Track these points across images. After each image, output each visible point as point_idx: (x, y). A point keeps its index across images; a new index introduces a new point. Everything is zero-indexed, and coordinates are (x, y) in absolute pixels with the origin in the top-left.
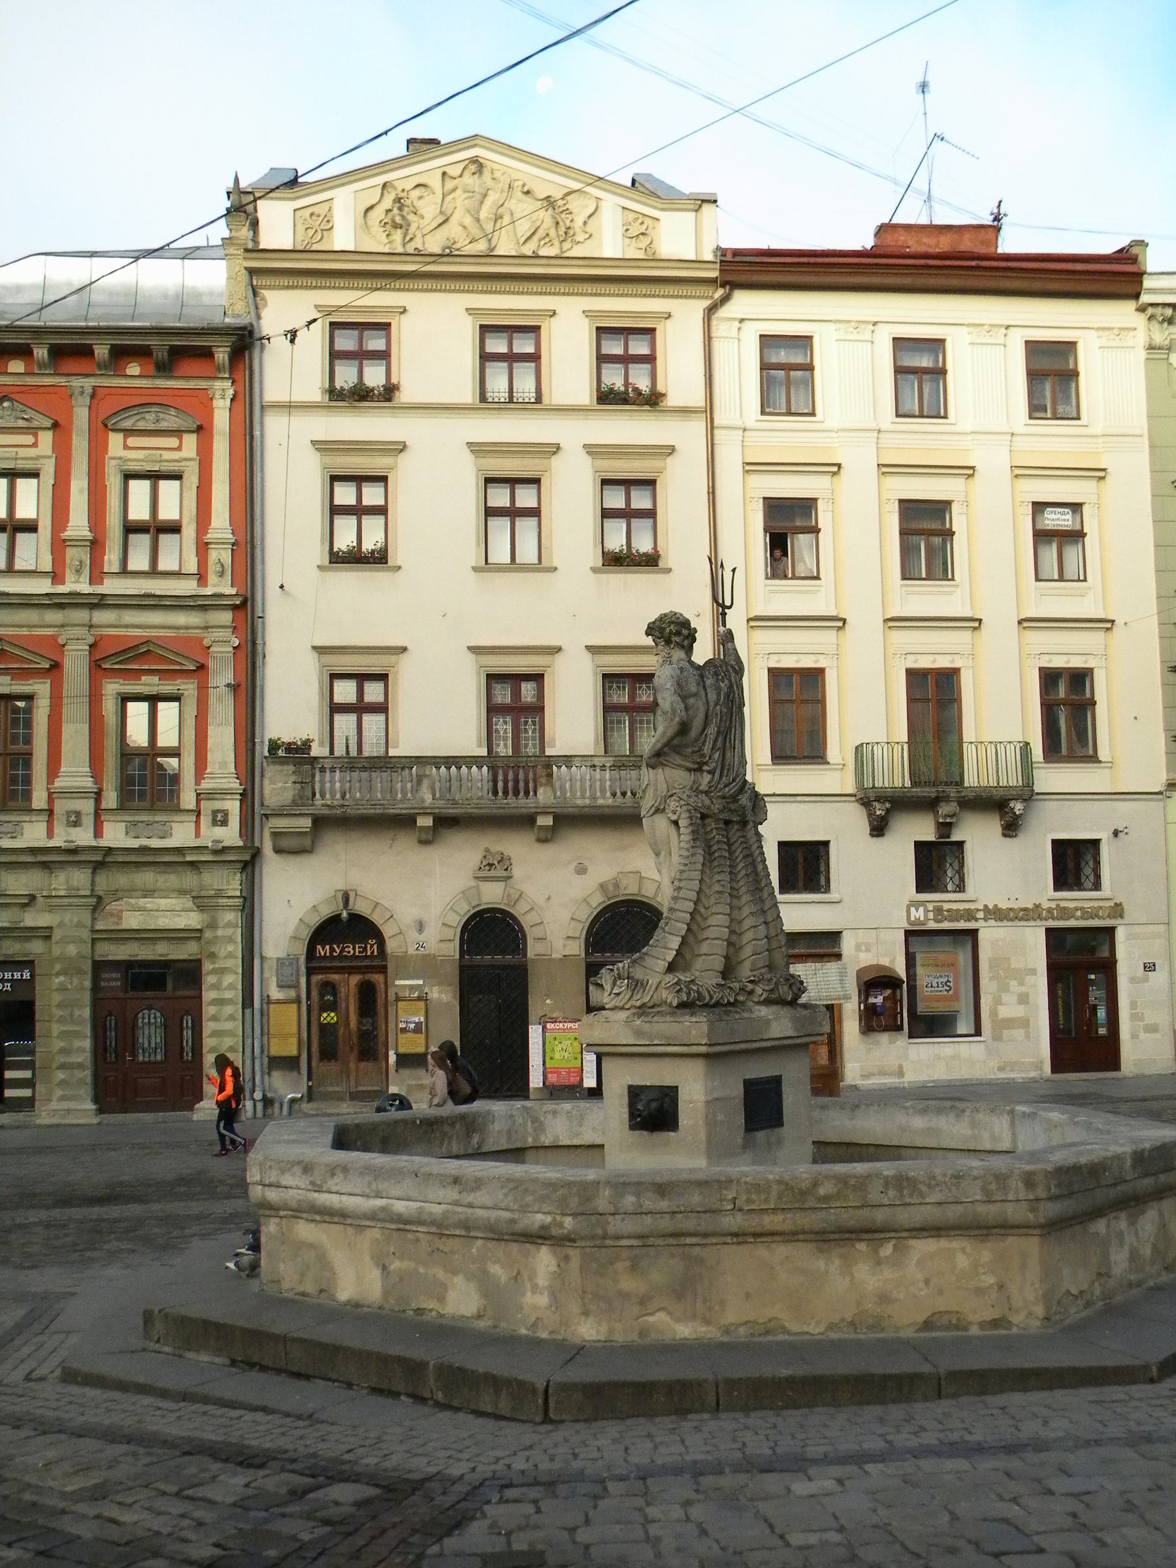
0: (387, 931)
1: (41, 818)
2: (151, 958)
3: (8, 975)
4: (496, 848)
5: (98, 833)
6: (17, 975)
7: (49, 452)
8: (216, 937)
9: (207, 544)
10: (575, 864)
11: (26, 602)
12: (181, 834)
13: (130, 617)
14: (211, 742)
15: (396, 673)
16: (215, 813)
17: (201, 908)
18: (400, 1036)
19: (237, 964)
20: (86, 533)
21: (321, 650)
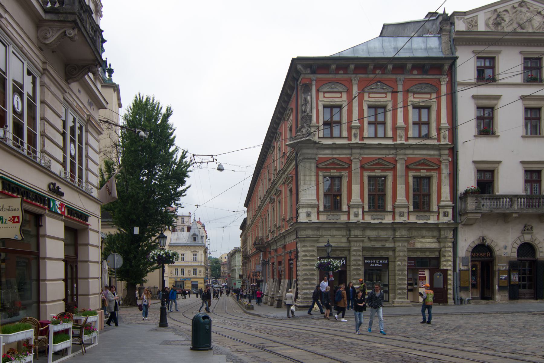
0: (496, 249)
1: (391, 214)
2: (424, 256)
3: (381, 261)
4: (529, 224)
5: (408, 219)
6: (384, 262)
7: (390, 99)
8: (446, 250)
9: (441, 128)
12: (433, 220)
13: (416, 152)
14: (442, 191)
15: (498, 170)
16: (445, 212)
17: (439, 242)
18: (500, 281)
19: (451, 258)
20: (403, 125)
21: (475, 162)
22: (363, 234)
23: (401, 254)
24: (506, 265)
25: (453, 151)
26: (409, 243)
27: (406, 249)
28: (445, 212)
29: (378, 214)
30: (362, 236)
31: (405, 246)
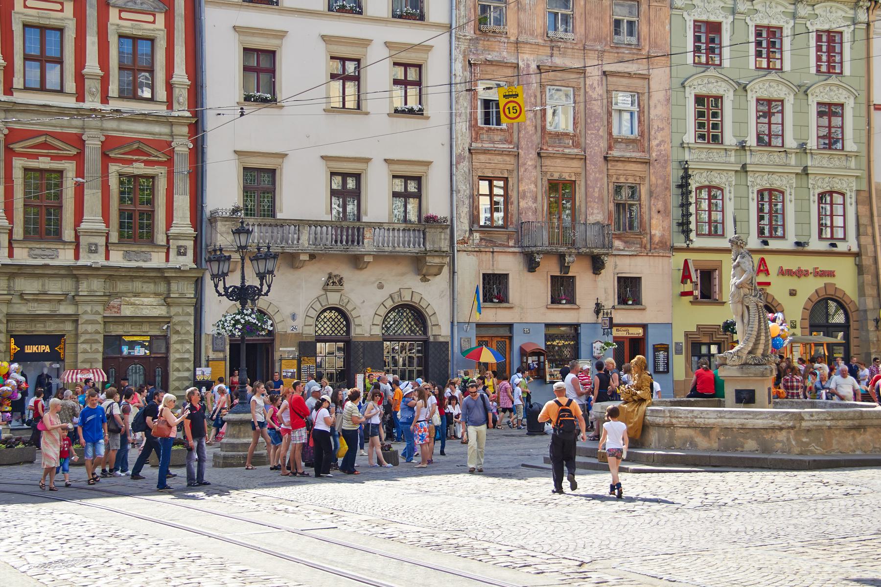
1: (71, 247)
4: (335, 273)
5: (107, 258)
10: (377, 283)
11: (62, 112)
12: (157, 260)
15: (281, 169)
17: (168, 305)
19: (191, 338)
22: (9, 287)
23: (90, 328)
24: (294, 349)
25: (197, 128)
26: (107, 306)
27: (99, 318)
28: (179, 247)
29: (42, 246)
30: (5, 292)
31: (97, 313)
